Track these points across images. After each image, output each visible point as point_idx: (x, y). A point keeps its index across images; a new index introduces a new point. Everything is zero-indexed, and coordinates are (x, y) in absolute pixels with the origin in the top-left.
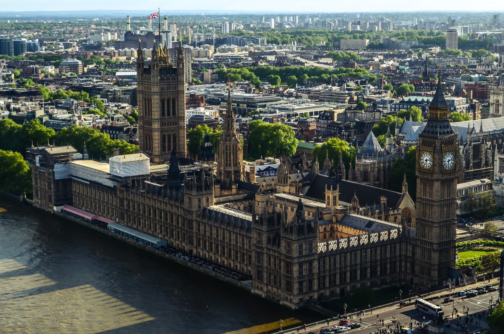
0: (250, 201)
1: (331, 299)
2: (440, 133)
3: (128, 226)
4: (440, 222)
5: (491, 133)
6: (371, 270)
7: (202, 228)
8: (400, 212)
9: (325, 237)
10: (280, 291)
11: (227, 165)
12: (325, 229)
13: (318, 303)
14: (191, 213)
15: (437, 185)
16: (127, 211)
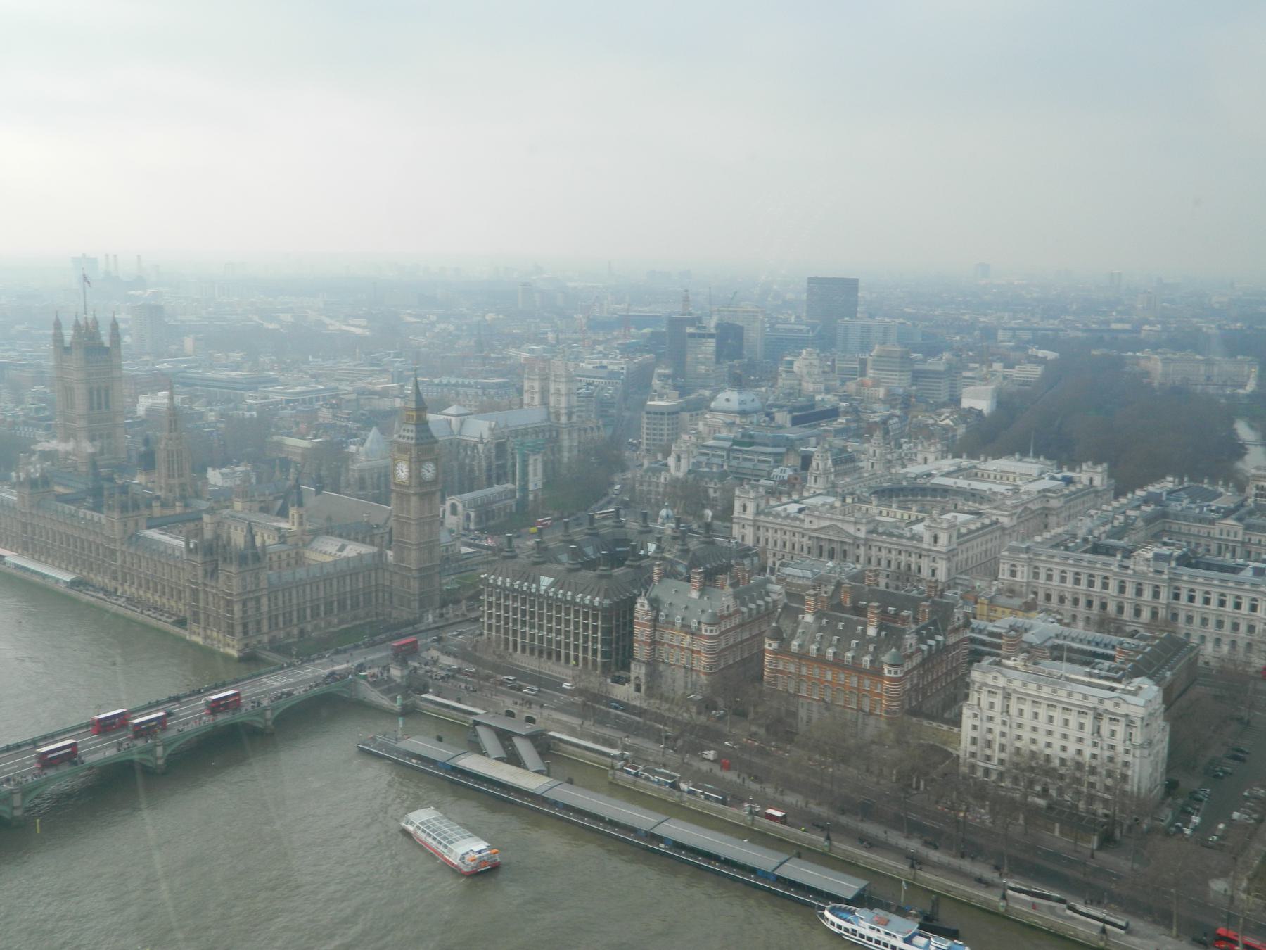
0: (197, 523)
1: (286, 642)
2: (417, 439)
3: (33, 558)
4: (420, 544)
5: (523, 427)
6: (339, 604)
7: (128, 559)
8: (387, 530)
9: (288, 565)
10: (221, 637)
11: (169, 476)
12: (288, 555)
13: (268, 648)
14: (114, 540)
15: (414, 500)
16: (33, 539)
